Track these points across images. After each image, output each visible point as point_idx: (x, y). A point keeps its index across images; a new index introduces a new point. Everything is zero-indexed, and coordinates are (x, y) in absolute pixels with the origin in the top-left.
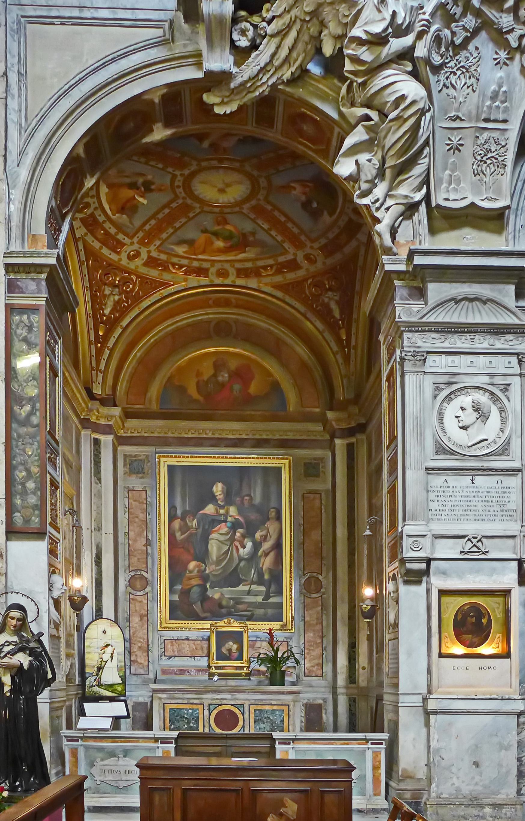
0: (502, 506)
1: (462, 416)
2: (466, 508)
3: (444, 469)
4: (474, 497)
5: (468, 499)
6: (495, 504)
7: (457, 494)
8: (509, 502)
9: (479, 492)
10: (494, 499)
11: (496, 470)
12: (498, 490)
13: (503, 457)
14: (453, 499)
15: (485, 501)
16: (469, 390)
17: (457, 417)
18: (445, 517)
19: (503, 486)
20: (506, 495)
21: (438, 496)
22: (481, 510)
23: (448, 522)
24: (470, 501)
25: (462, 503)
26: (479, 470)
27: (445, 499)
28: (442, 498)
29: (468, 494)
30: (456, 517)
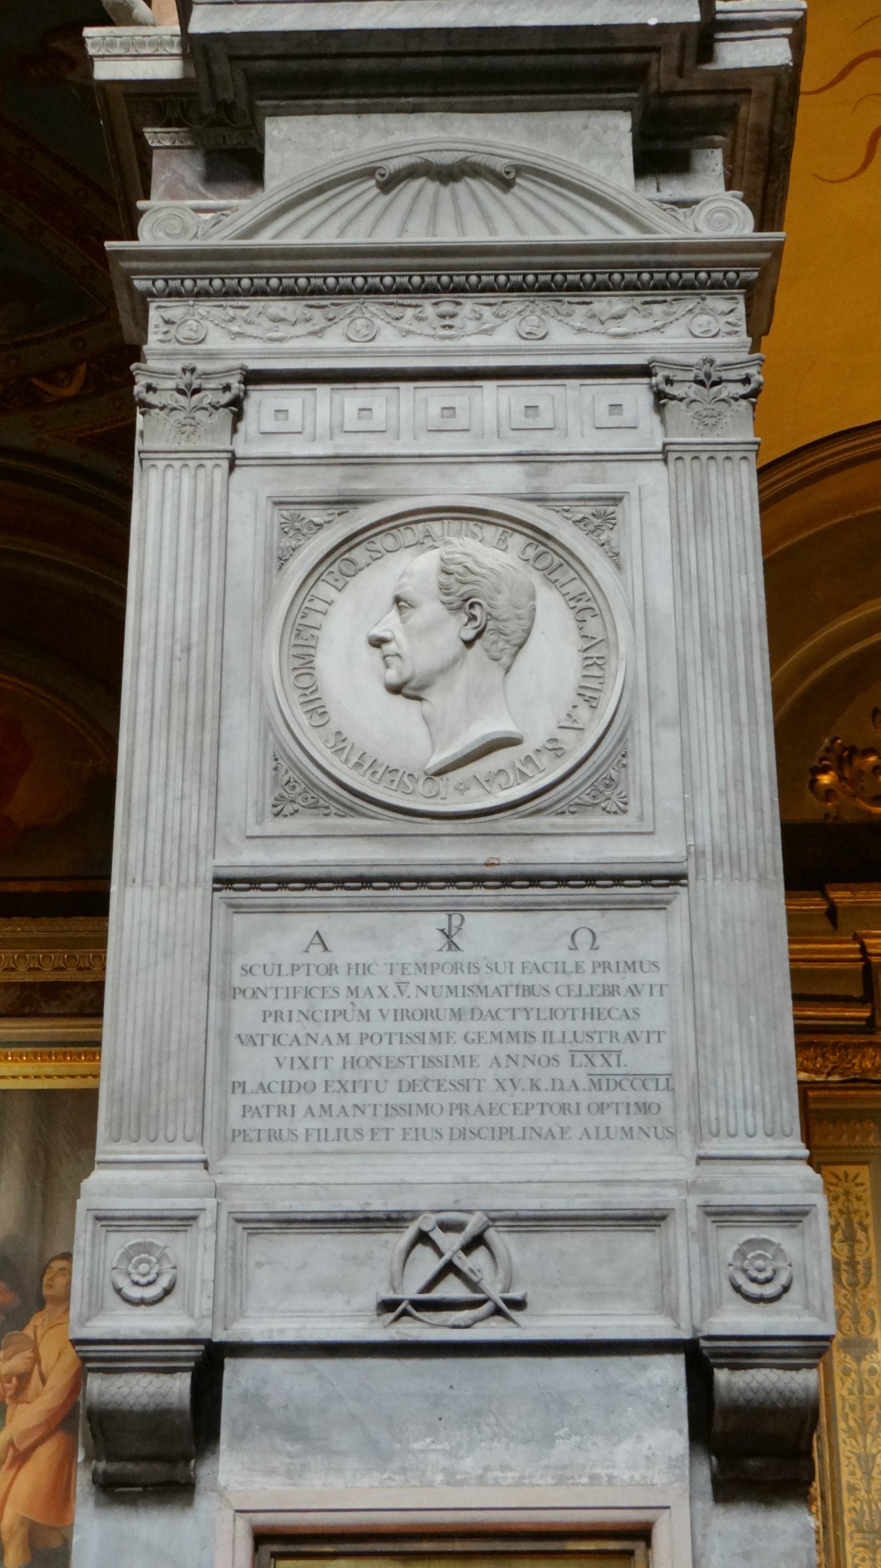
0: (598, 1060)
1: (400, 635)
2: (418, 1073)
3: (311, 883)
4: (457, 1014)
5: (430, 1026)
6: (561, 1051)
7: (374, 1005)
8: (632, 1037)
9: (483, 990)
10: (557, 1027)
11: (562, 880)
12: (576, 980)
13: (597, 820)
14: (354, 1028)
15: (513, 1036)
16: (436, 528)
17: (378, 643)
18: (313, 1124)
19: (600, 956)
20: (619, 1002)
21: (278, 1015)
22: (490, 1084)
23: (323, 1146)
24: (436, 1038)
25: (397, 1050)
26: (478, 880)
27: (311, 1027)
28: (296, 1027)
29: (428, 1002)
30: (365, 1122)
